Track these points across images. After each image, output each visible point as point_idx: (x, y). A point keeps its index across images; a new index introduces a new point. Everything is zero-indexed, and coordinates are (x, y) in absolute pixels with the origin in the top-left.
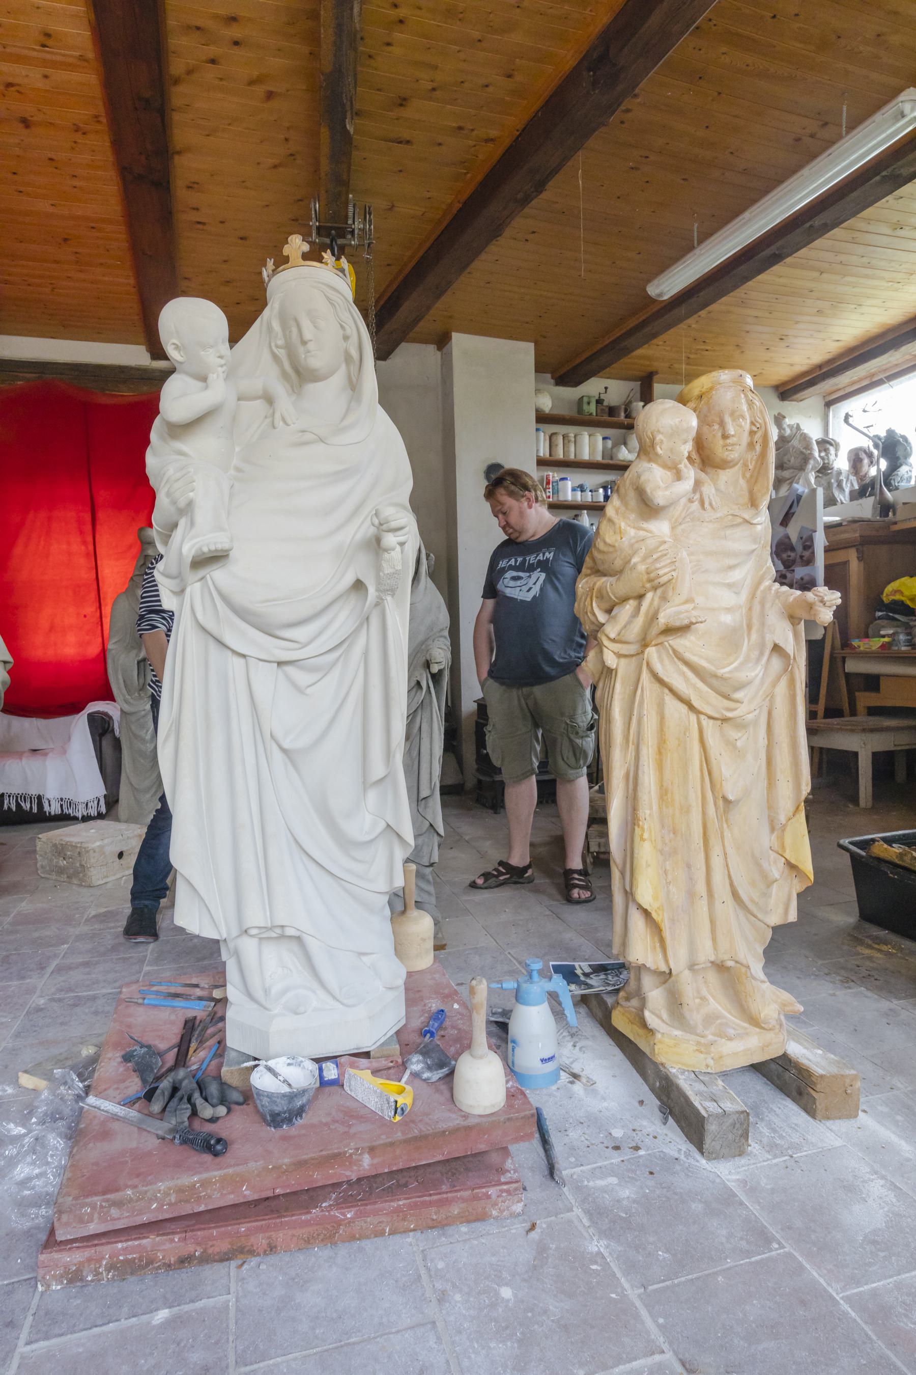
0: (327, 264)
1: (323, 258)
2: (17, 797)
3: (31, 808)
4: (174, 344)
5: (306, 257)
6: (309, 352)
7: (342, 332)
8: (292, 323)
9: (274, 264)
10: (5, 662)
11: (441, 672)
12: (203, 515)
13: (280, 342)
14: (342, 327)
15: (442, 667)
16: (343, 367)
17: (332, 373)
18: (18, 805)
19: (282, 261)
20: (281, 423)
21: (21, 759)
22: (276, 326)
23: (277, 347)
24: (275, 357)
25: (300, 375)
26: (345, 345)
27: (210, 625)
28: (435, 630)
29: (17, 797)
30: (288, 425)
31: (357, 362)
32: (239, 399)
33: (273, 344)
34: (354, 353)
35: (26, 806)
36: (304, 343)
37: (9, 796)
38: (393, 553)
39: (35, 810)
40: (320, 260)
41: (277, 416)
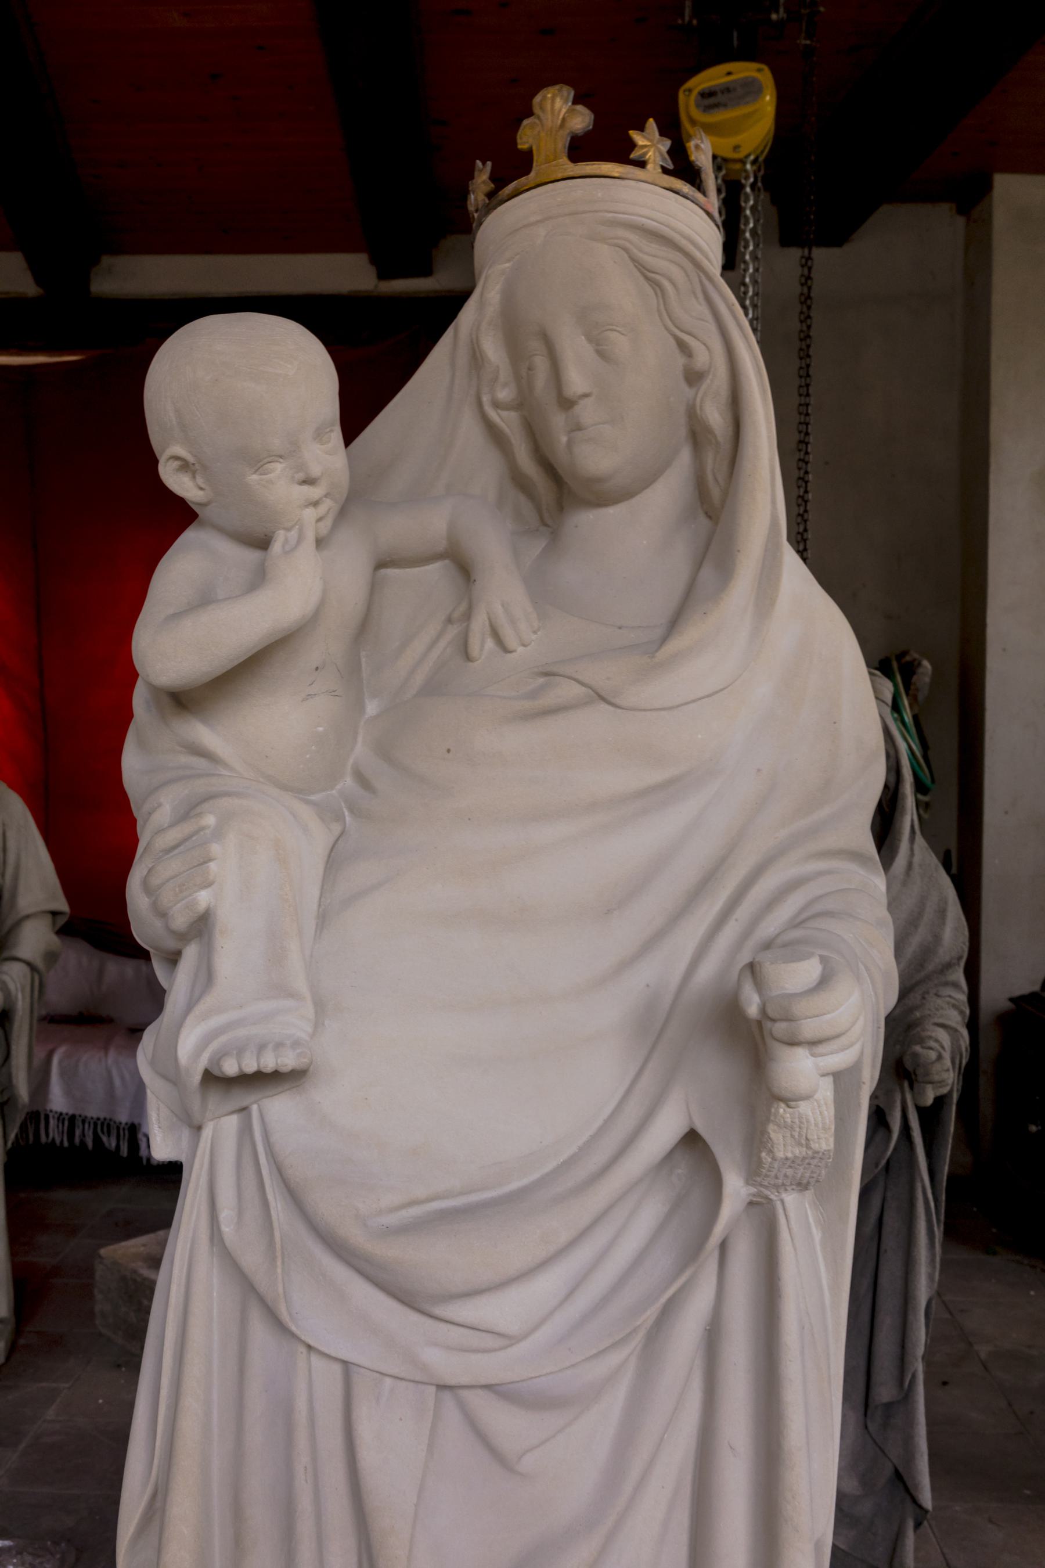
0: (641, 164)
1: (633, 145)
2: (95, 1124)
3: (118, 1146)
4: (176, 458)
5: (582, 149)
6: (579, 428)
7: (681, 360)
8: (535, 345)
9: (493, 178)
10: (54, 914)
11: (940, 1101)
12: (235, 955)
13: (504, 394)
14: (682, 346)
15: (945, 1091)
16: (685, 456)
17: (647, 481)
18: (97, 1139)
19: (514, 168)
20: (490, 644)
21: (106, 1049)
22: (493, 350)
23: (497, 405)
24: (495, 435)
25: (552, 491)
26: (688, 392)
27: (252, 1259)
28: (930, 967)
29: (95, 1124)
30: (506, 650)
31: (726, 446)
32: (381, 565)
33: (486, 399)
34: (715, 417)
35: (110, 1143)
36: (567, 404)
37: (83, 1122)
38: (804, 1107)
39: (124, 1151)
40: (622, 152)
41: (479, 623)
